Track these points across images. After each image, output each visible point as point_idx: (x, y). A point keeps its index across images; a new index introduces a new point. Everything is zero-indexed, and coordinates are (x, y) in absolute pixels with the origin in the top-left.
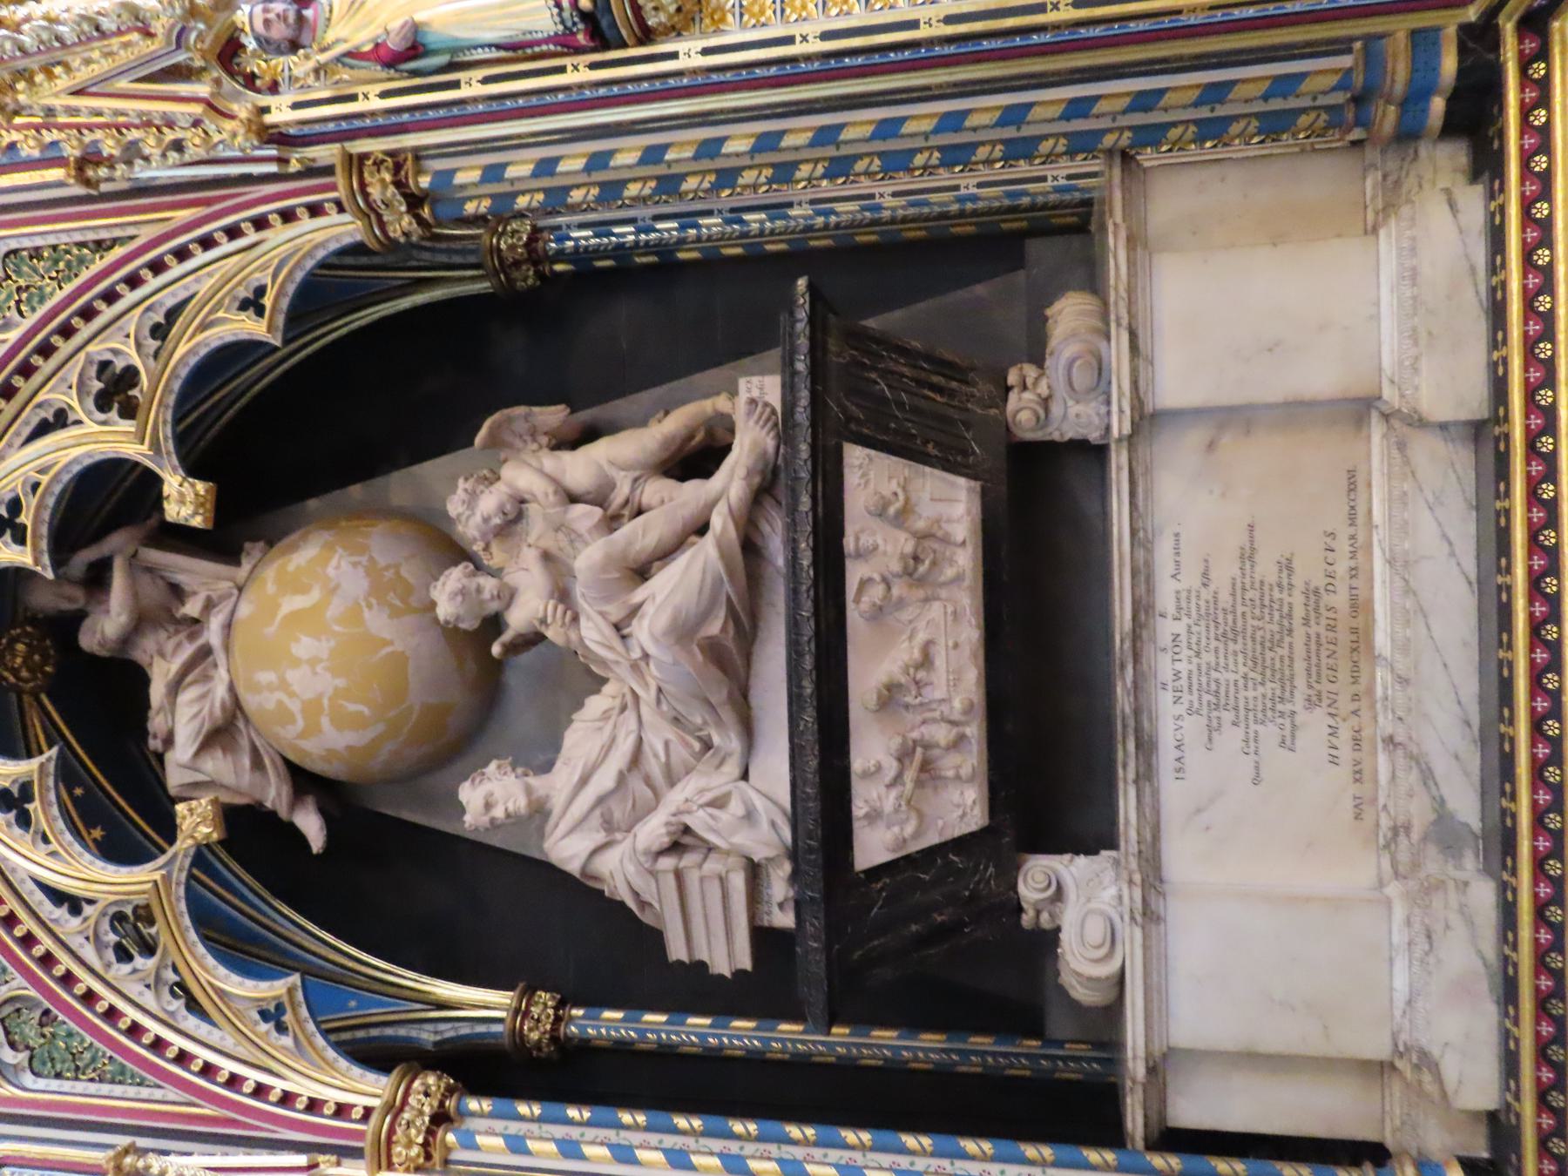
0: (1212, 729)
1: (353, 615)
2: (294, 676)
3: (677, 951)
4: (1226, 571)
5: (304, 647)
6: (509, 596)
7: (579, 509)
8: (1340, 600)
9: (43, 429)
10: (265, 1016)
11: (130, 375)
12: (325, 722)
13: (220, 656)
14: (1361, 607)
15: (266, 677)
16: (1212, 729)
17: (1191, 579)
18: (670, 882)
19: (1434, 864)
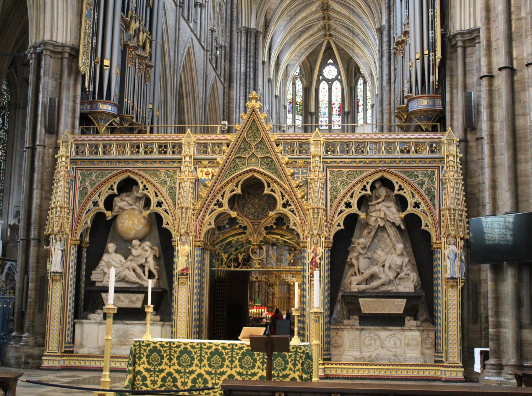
0: (115, 330)
1: (134, 229)
2: (127, 221)
3: (93, 272)
4: (131, 332)
5: (130, 223)
6: (136, 249)
7: (145, 260)
8: (127, 343)
9: (156, 193)
10: (86, 222)
11: (161, 206)
12: (121, 224)
13: (130, 207)
14: (126, 345)
15: (127, 216)
16: (115, 330)
17: (130, 329)
18: (100, 272)
19: (101, 350)
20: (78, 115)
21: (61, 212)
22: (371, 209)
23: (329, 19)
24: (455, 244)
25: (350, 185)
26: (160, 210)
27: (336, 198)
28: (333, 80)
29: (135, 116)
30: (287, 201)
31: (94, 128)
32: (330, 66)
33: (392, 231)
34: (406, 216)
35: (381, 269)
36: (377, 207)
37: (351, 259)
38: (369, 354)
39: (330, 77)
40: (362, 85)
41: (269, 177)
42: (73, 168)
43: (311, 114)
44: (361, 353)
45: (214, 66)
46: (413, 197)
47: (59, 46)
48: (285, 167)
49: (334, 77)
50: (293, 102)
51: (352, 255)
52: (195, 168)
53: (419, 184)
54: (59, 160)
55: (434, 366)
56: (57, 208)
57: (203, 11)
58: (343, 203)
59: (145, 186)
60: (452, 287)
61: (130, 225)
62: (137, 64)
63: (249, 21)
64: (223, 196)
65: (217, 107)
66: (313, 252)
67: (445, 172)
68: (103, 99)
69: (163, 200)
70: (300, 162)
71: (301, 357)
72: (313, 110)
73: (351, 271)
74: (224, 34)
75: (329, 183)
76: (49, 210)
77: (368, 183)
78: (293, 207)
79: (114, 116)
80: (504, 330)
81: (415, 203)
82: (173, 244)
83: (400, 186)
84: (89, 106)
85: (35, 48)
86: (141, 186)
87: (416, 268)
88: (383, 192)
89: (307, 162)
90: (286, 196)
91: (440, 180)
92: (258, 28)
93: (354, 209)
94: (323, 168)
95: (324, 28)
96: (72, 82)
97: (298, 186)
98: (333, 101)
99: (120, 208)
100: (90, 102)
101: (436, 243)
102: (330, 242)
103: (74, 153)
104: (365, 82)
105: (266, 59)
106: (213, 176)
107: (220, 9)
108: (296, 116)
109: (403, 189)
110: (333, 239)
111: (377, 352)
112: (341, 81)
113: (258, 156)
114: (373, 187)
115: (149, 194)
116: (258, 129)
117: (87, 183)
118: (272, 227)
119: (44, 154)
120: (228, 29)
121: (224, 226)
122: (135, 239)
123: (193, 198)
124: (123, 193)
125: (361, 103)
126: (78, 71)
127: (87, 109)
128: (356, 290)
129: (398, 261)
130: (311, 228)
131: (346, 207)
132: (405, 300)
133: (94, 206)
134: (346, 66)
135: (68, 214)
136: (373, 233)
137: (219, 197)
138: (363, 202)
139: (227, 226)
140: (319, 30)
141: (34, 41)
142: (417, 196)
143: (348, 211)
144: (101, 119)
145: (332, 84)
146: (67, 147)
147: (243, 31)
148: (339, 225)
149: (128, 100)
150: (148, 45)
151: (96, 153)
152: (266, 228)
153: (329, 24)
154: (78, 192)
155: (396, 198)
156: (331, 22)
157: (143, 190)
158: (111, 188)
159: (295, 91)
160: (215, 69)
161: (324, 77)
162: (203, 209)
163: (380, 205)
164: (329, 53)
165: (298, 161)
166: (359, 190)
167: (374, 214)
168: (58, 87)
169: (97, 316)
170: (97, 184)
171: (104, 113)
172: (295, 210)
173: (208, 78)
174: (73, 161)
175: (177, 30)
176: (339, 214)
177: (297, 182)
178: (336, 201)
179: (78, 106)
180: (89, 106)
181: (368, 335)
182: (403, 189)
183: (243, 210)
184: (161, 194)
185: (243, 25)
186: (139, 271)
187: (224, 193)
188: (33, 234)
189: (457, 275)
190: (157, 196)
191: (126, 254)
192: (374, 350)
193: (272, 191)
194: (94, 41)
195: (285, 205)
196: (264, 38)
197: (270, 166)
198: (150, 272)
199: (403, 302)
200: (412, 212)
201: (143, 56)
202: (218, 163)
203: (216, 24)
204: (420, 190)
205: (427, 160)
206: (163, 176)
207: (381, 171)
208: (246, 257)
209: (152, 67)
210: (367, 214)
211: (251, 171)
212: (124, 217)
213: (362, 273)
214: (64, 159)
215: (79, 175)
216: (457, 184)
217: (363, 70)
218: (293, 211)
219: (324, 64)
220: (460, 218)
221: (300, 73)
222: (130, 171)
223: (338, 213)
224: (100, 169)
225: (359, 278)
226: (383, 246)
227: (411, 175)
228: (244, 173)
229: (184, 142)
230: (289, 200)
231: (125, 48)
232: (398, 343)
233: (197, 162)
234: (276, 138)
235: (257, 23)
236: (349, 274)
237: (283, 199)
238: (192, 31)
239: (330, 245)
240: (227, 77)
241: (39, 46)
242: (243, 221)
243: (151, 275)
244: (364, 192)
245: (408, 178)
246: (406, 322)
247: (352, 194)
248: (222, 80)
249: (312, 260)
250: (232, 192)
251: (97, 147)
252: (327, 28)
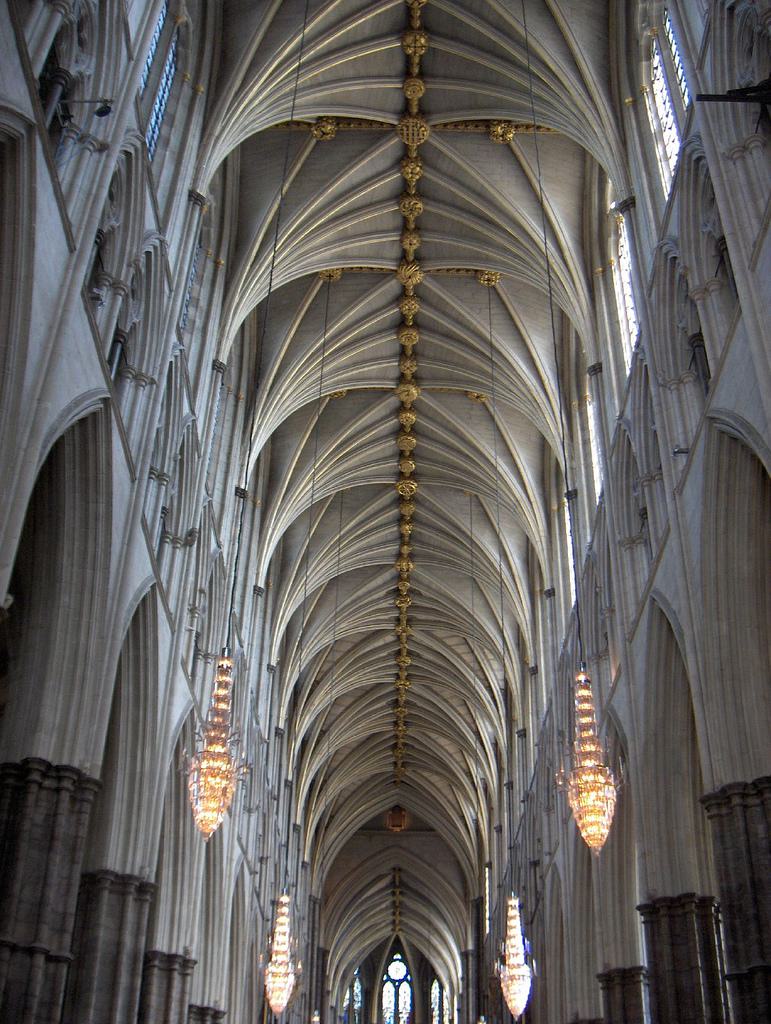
28: (401, 981)
39: (397, 978)
40: (438, 990)
95: (394, 922)
98: (401, 1008)
104: (441, 987)
125: (436, 1013)
161: (388, 976)
164: (397, 947)
217: (441, 972)
219: (391, 960)
235: (326, 942)
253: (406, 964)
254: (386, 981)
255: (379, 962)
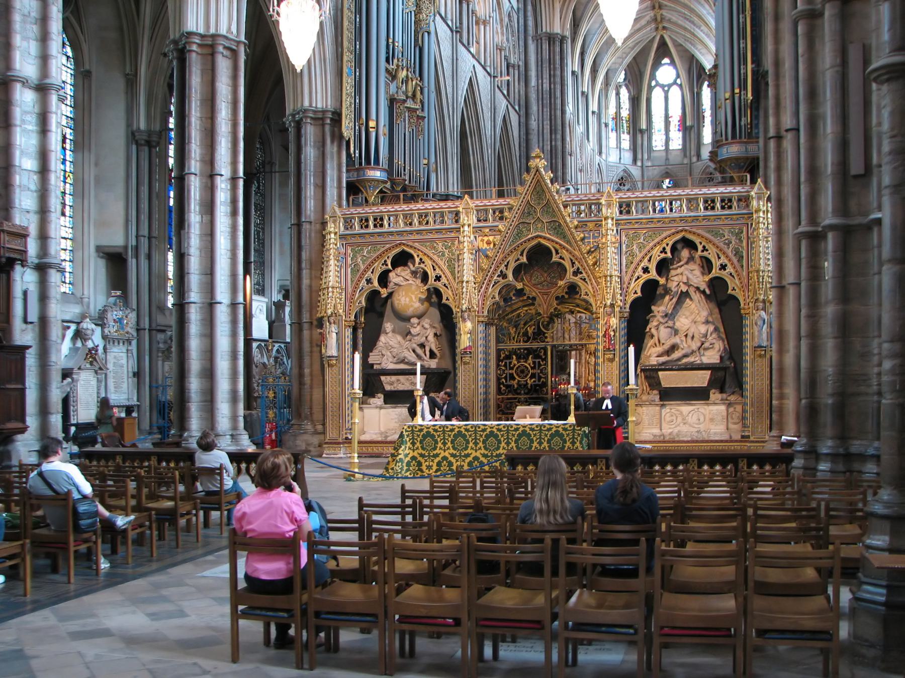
3: (371, 354)
5: (408, 299)
9: (433, 267)
20: (344, 185)
21: (333, 292)
22: (673, 273)
23: (660, 7)
24: (764, 309)
25: (648, 248)
26: (439, 285)
27: (632, 263)
28: (670, 86)
29: (407, 178)
30: (578, 269)
31: (362, 198)
32: (666, 66)
33: (696, 296)
34: (711, 280)
35: (684, 338)
36: (679, 271)
37: (650, 329)
38: (670, 431)
39: (666, 83)
41: (557, 243)
42: (343, 244)
43: (641, 131)
44: (661, 430)
45: (505, 92)
46: (719, 258)
47: (320, 111)
48: (574, 231)
49: (671, 81)
50: (617, 117)
51: (653, 324)
52: (475, 237)
53: (725, 244)
54: (328, 237)
55: (741, 441)
56: (328, 288)
57: (488, 28)
58: (640, 269)
59: (421, 259)
60: (760, 356)
61: (407, 302)
62: (407, 118)
63: (552, 24)
64: (506, 266)
65: (512, 143)
66: (606, 323)
67: (754, 229)
68: (370, 164)
69: (441, 273)
70: (591, 225)
71: (579, 435)
72: (644, 127)
73: (651, 342)
74: (517, 50)
75: (624, 246)
76: (320, 290)
77: (667, 245)
78: (584, 274)
79: (385, 182)
80: (786, 401)
81: (721, 265)
82: (455, 321)
83: (704, 247)
84: (355, 174)
85: (293, 116)
86: (417, 260)
87: (724, 336)
88: (685, 253)
89: (598, 224)
90: (577, 263)
91: (748, 238)
92: (563, 32)
93: (653, 274)
94: (617, 230)
95: (655, 20)
96: (335, 149)
97: (589, 252)
99: (396, 284)
100: (357, 169)
101: (744, 309)
102: (626, 312)
103: (342, 228)
105: (576, 68)
106: (494, 245)
107: (510, 20)
108: (622, 135)
109: (707, 250)
110: (630, 308)
111: (678, 428)
112: (680, 86)
113: (544, 221)
114: (674, 249)
115: (426, 268)
116: (543, 191)
117: (359, 260)
118: (563, 296)
119: (310, 230)
120: (522, 43)
121: (511, 298)
122: (413, 317)
123: (473, 270)
124: (397, 267)
126: (341, 136)
127: (354, 177)
128: (655, 363)
129: (703, 329)
130: (604, 298)
131: (644, 273)
132: (710, 372)
133: (367, 284)
134: (687, 67)
135: (340, 294)
136: (675, 300)
137: (502, 267)
138: (663, 267)
139: (514, 298)
140: (648, 23)
141: (292, 107)
142: (722, 257)
143: (646, 277)
144: (370, 187)
145: (668, 91)
146: (334, 222)
147: (543, 38)
148: (636, 293)
149: (398, 161)
150: (418, 93)
151: (367, 227)
152: (557, 298)
153: (662, 15)
154: (349, 270)
155: (701, 260)
156: (664, 13)
157: (419, 264)
158: (385, 263)
159: (620, 103)
160: (506, 97)
161: (657, 82)
162: (486, 282)
163: (683, 268)
164: (663, 50)
165: (588, 224)
166: (658, 253)
167: (675, 278)
168: (321, 156)
169: (379, 400)
170: (370, 260)
171: (374, 180)
172: (586, 277)
173: (497, 111)
174: (343, 237)
175: (455, 60)
176: (636, 280)
177: (588, 248)
178: (633, 266)
179: (344, 175)
180: (355, 174)
181: (668, 411)
182: (707, 250)
183: (531, 279)
184: (439, 267)
185: (544, 30)
186: (419, 351)
187: (508, 263)
188: (306, 317)
189: (765, 344)
190: (434, 270)
191: (407, 334)
192: (676, 427)
193: (561, 258)
194: (357, 101)
195: (576, 273)
196: (574, 40)
197: (558, 231)
198: (431, 351)
199: (707, 374)
200: (717, 275)
201: (413, 108)
202: (500, 231)
203: (505, 40)
204: (726, 249)
205: (734, 217)
206: (440, 246)
207: (682, 231)
208: (536, 331)
209: (425, 117)
210: (667, 280)
211: (537, 237)
212: (401, 293)
213: (663, 344)
214: (333, 236)
215: (349, 251)
216: (767, 242)
218: (584, 280)
219: (657, 64)
220: (770, 280)
221: (625, 80)
222: (404, 244)
223: (634, 279)
224: (374, 244)
225: (659, 349)
226: (687, 313)
227: (716, 234)
228: (529, 240)
229: (461, 210)
230: (580, 267)
231: (392, 101)
232: (702, 419)
233: (477, 230)
234: (564, 200)
235: (563, 27)
236: (649, 345)
237: (573, 267)
238: (473, 56)
239: (626, 315)
240: (523, 103)
241: (298, 113)
242: (531, 291)
243: (432, 355)
244: (663, 255)
245: (712, 238)
246: (711, 395)
247: (651, 258)
248: (517, 108)
249: (605, 332)
250: (516, 261)
251: (367, 220)
252: (659, 19)
253: (675, 67)
254: (655, 86)
255: (645, 65)
